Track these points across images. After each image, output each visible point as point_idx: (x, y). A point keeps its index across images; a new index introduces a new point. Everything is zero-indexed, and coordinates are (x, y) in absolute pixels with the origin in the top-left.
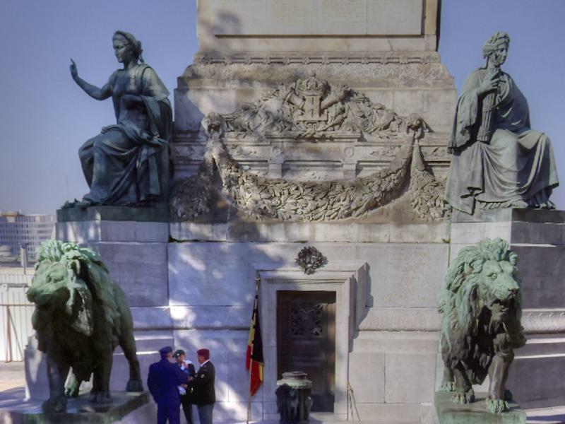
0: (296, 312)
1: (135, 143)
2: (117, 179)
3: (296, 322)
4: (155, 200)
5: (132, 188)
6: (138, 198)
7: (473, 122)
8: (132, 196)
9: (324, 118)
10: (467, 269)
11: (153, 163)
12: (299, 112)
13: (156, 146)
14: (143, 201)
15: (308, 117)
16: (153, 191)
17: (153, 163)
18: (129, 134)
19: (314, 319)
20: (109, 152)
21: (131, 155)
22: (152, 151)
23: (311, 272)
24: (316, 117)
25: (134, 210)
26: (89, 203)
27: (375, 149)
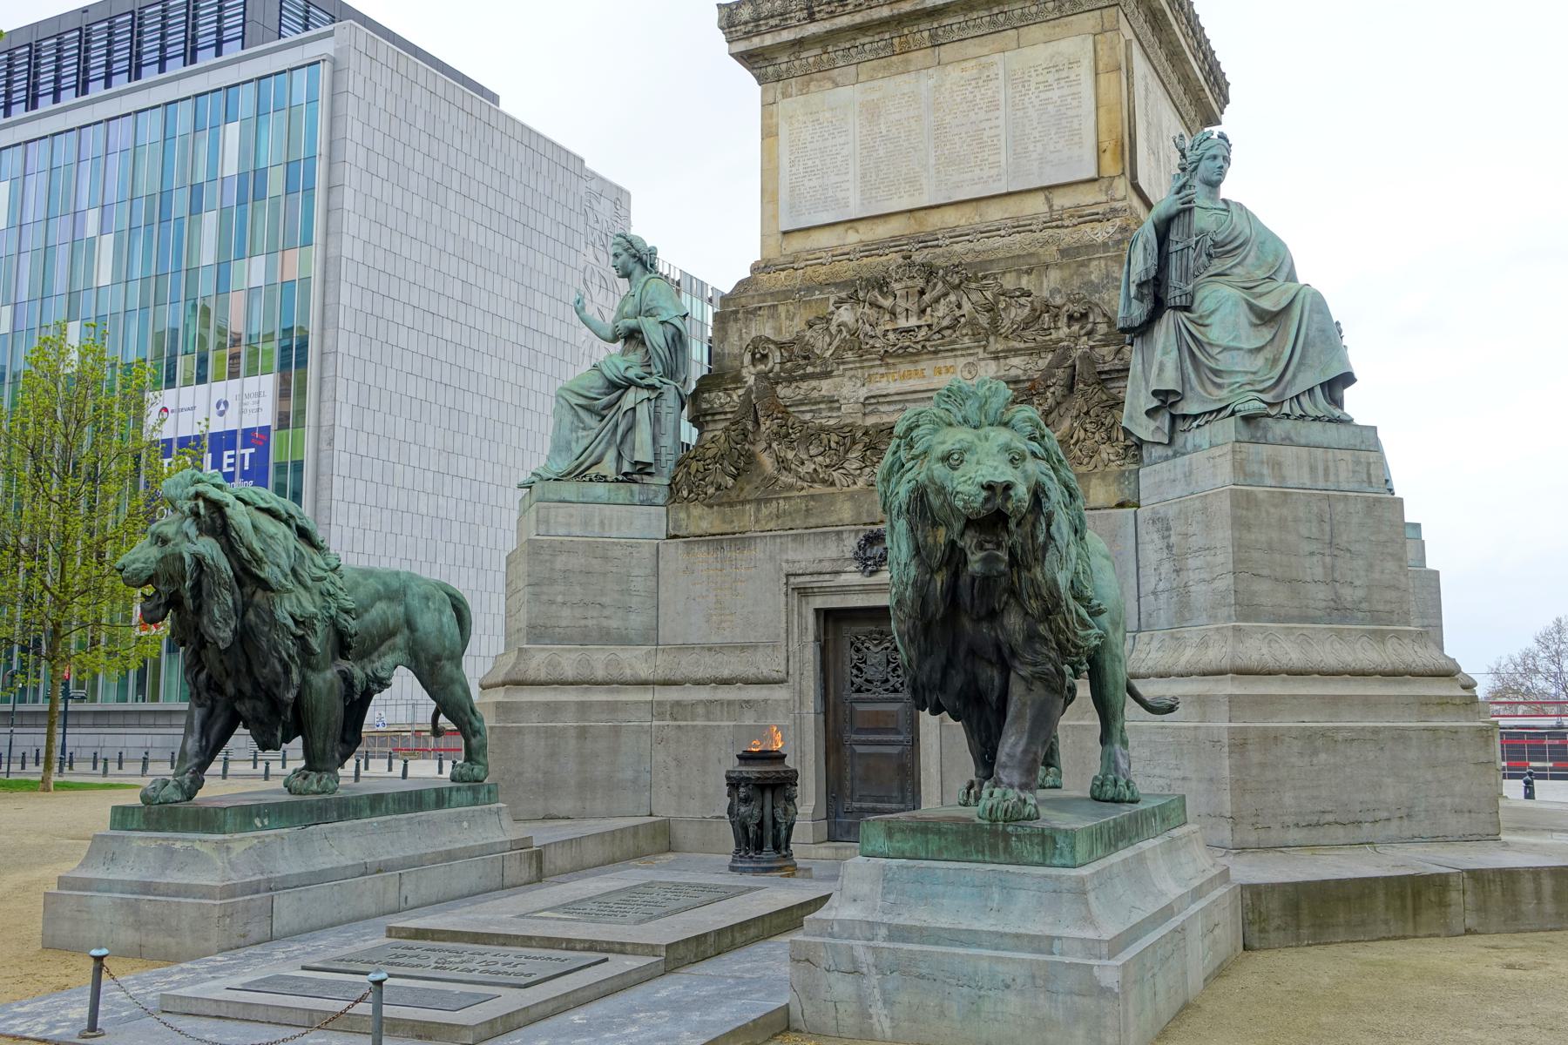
0: (858, 650)
1: (618, 386)
2: (586, 442)
3: (859, 669)
4: (640, 472)
5: (611, 455)
6: (618, 470)
7: (1153, 273)
8: (608, 467)
9: (927, 319)
11: (643, 412)
12: (887, 317)
13: (651, 387)
14: (625, 474)
15: (902, 323)
16: (644, 454)
17: (643, 412)
18: (607, 373)
19: (889, 662)
20: (575, 400)
21: (609, 406)
22: (645, 394)
23: (872, 573)
24: (913, 322)
25: (600, 489)
27: (1016, 361)
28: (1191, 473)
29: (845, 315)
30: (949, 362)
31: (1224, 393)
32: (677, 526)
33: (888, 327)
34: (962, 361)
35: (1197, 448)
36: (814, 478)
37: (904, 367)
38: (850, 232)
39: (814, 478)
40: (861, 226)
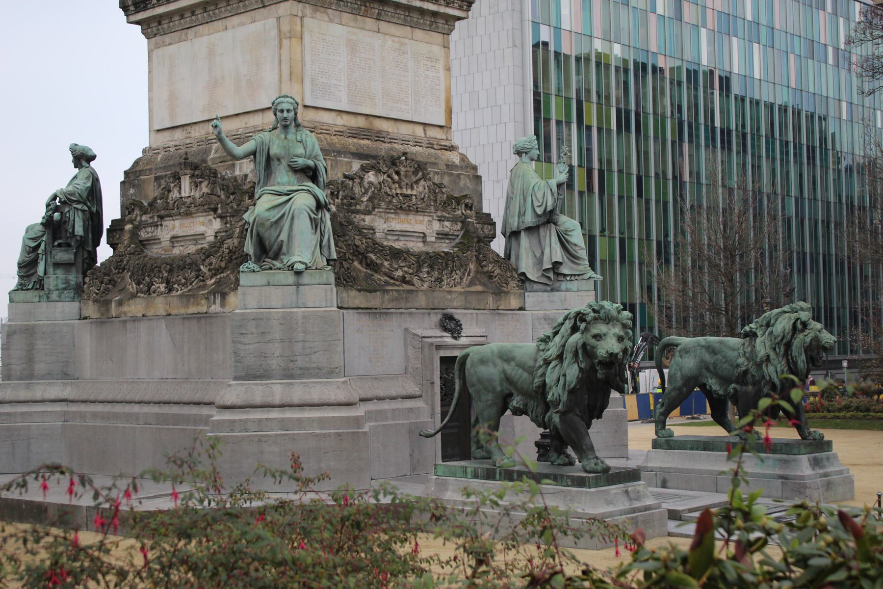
10: (799, 326)
12: (397, 186)
15: (405, 191)
24: (409, 192)
26: (304, 266)
27: (447, 224)
28: (565, 300)
29: (371, 177)
30: (421, 218)
31: (581, 267)
32: (342, 302)
33: (398, 192)
34: (427, 219)
35: (567, 290)
36: (403, 280)
37: (403, 217)
38: (339, 118)
39: (403, 280)
40: (345, 116)
